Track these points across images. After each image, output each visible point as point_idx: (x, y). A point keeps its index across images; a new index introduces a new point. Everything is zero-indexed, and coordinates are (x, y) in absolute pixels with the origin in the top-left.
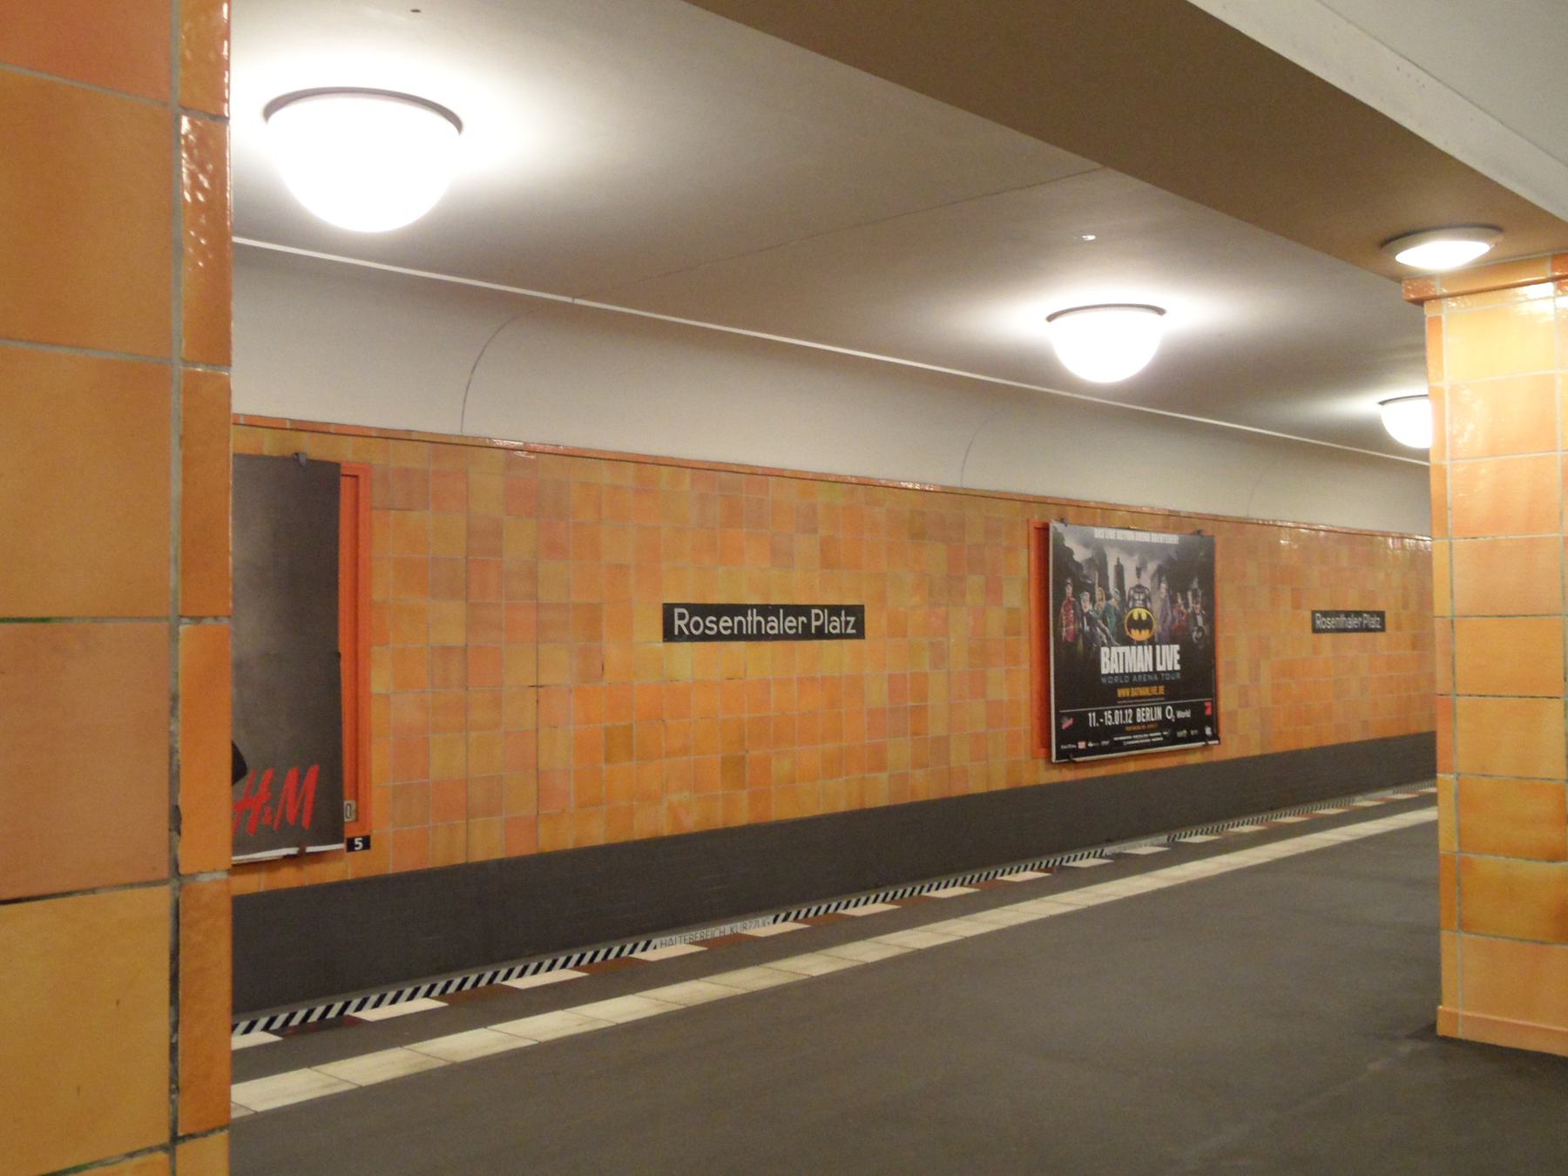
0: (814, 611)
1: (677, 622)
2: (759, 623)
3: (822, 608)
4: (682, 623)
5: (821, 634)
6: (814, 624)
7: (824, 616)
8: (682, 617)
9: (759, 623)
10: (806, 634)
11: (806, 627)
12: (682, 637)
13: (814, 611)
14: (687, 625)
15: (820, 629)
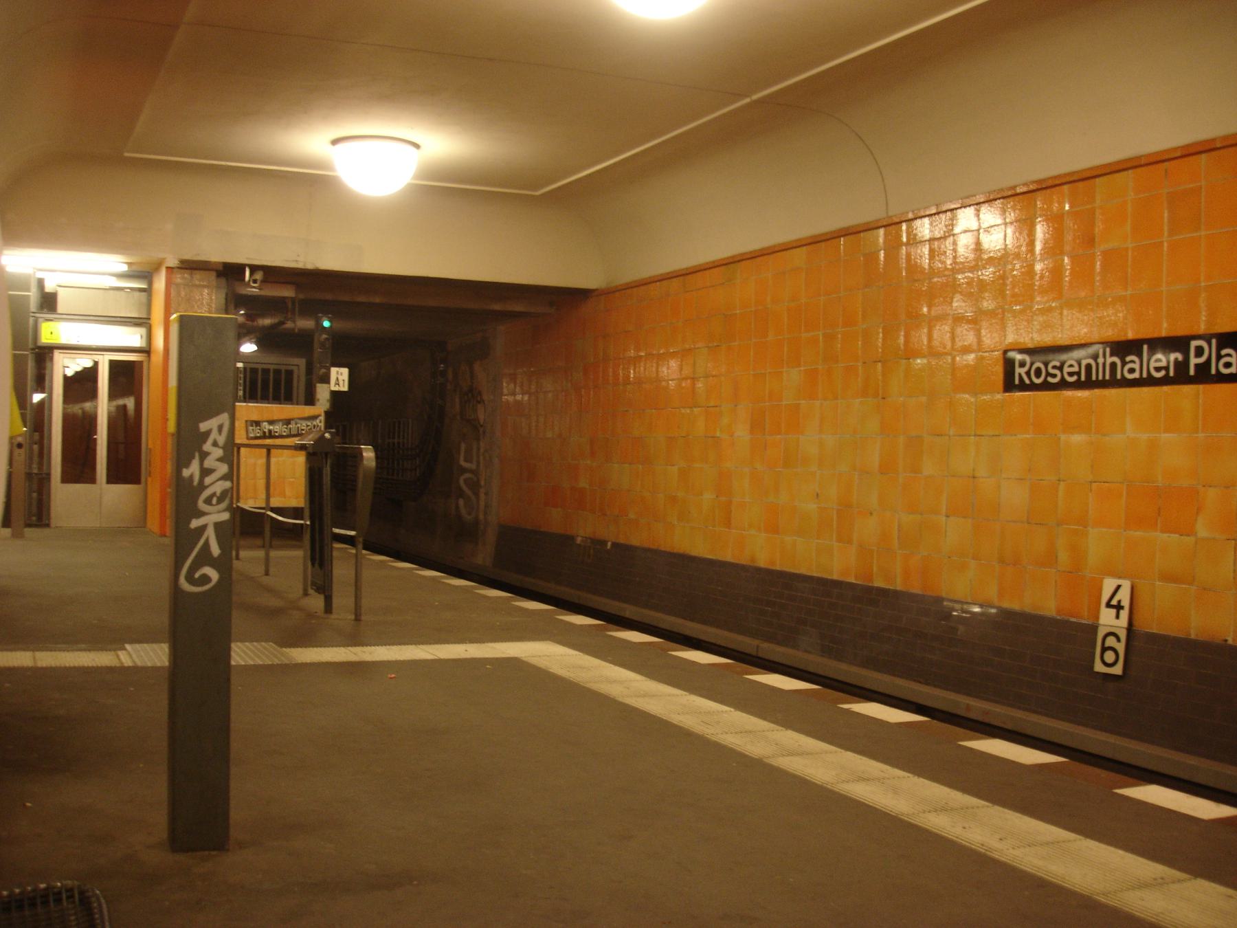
0: (1194, 344)
1: (1018, 370)
2: (1113, 365)
3: (1207, 338)
4: (1023, 371)
5: (1204, 375)
6: (1194, 361)
7: (1210, 350)
8: (1022, 364)
9: (1113, 365)
10: (1180, 376)
11: (1182, 366)
12: (1023, 387)
13: (1194, 344)
14: (1028, 373)
15: (1203, 369)
